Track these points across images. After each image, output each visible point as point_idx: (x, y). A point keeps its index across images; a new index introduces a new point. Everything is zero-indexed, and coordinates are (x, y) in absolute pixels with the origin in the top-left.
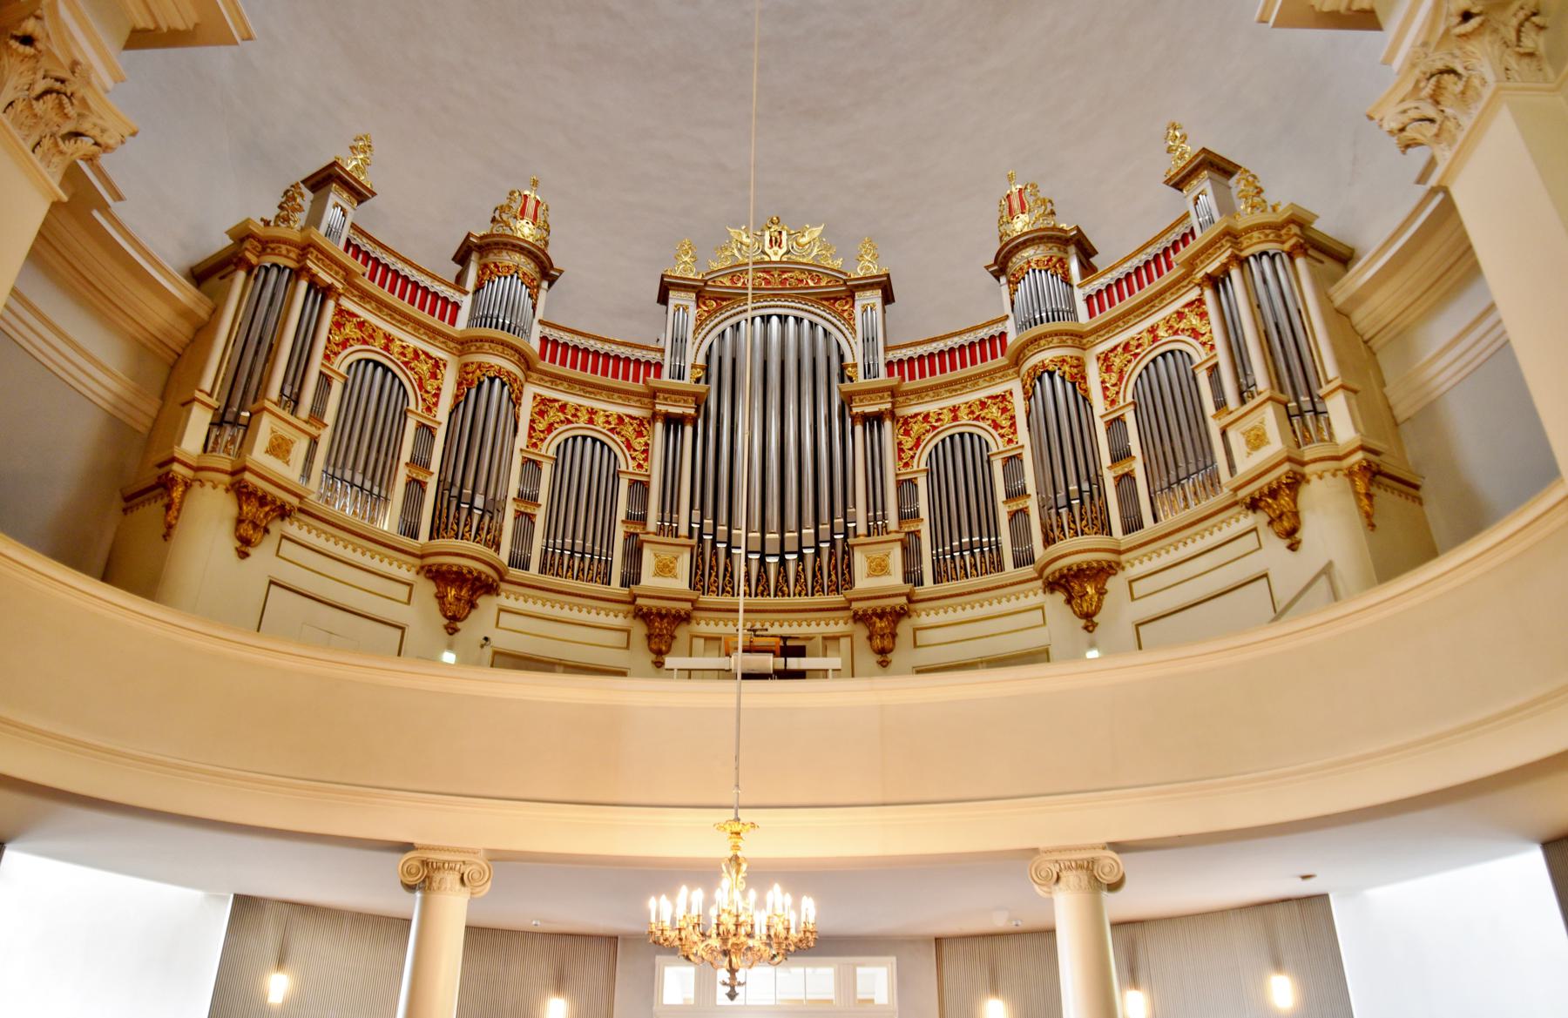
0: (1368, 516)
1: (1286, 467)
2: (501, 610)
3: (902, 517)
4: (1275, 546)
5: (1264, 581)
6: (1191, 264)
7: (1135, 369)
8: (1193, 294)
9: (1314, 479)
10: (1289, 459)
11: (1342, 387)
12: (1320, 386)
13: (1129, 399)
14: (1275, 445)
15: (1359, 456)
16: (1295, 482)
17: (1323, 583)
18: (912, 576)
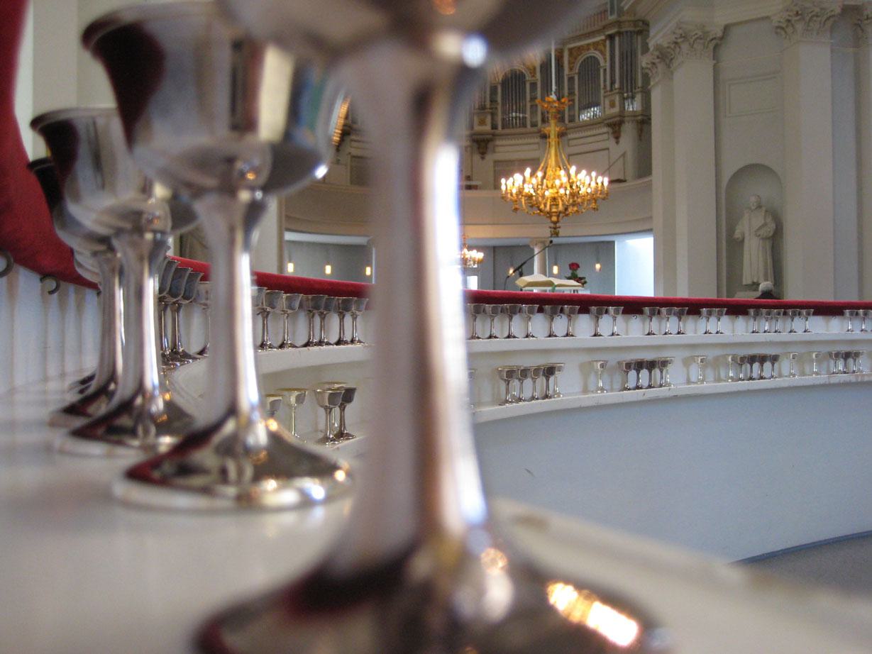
0: (640, 136)
1: (618, 119)
2: (352, 140)
3: (491, 101)
4: (613, 141)
5: (607, 152)
6: (604, 28)
7: (581, 59)
8: (603, 37)
9: (627, 123)
10: (620, 116)
11: (641, 92)
12: (635, 89)
13: (577, 71)
14: (616, 110)
15: (640, 118)
16: (620, 123)
17: (621, 159)
18: (494, 127)
